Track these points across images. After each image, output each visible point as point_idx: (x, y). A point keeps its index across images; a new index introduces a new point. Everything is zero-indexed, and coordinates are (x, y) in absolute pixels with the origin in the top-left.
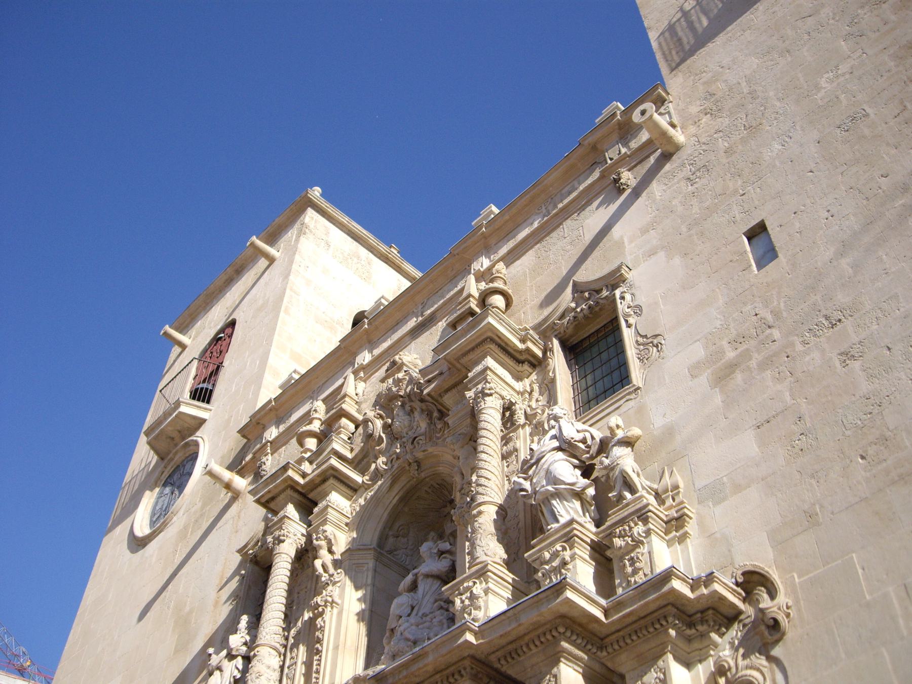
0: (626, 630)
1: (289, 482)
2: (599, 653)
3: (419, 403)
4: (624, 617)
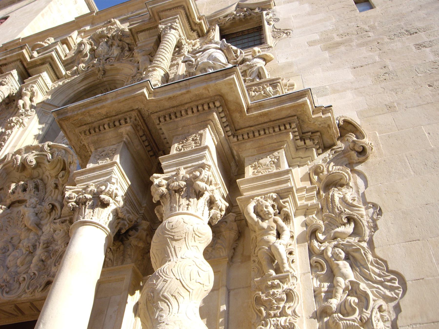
0: (257, 127)
2: (232, 137)
3: (118, 42)
4: (261, 115)
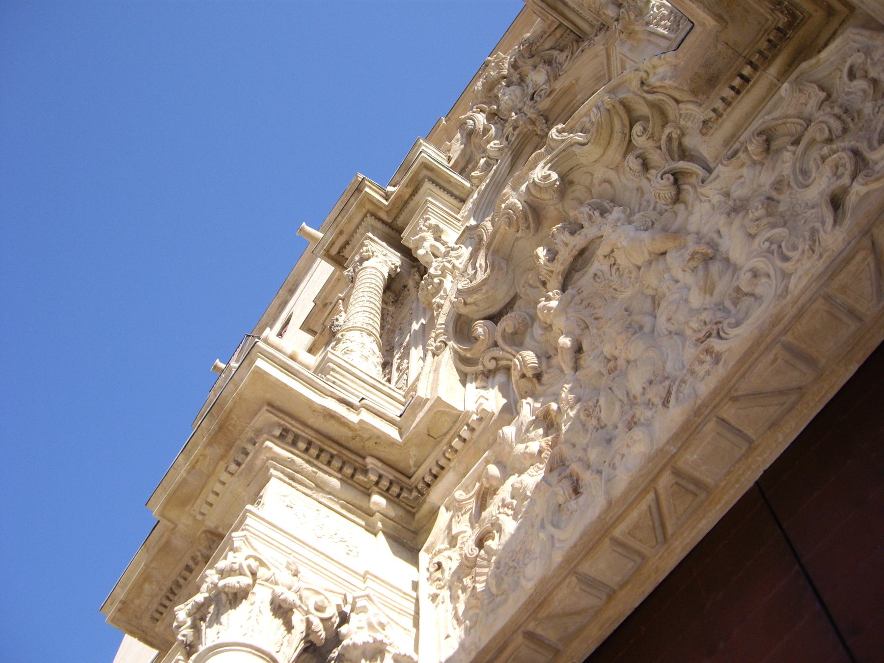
1: (369, 206)
3: (530, 62)
